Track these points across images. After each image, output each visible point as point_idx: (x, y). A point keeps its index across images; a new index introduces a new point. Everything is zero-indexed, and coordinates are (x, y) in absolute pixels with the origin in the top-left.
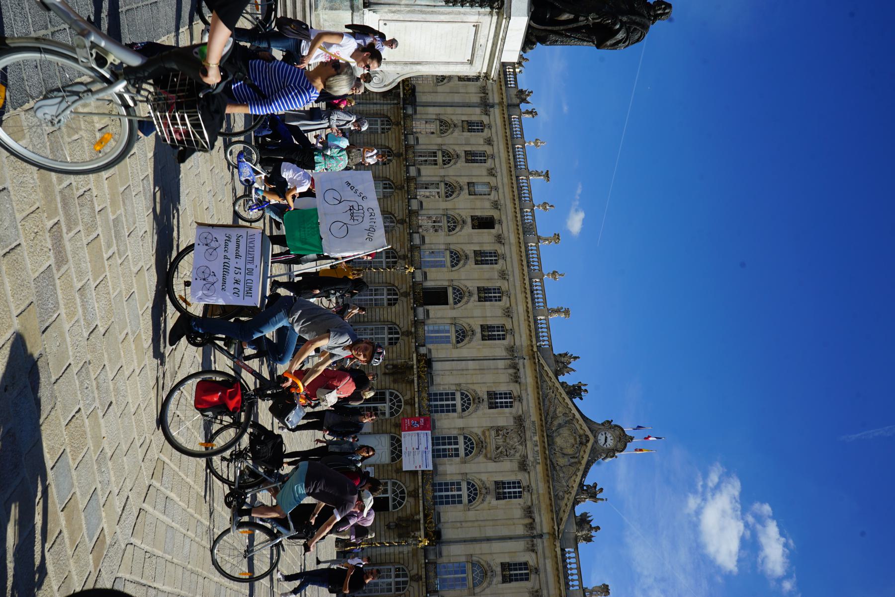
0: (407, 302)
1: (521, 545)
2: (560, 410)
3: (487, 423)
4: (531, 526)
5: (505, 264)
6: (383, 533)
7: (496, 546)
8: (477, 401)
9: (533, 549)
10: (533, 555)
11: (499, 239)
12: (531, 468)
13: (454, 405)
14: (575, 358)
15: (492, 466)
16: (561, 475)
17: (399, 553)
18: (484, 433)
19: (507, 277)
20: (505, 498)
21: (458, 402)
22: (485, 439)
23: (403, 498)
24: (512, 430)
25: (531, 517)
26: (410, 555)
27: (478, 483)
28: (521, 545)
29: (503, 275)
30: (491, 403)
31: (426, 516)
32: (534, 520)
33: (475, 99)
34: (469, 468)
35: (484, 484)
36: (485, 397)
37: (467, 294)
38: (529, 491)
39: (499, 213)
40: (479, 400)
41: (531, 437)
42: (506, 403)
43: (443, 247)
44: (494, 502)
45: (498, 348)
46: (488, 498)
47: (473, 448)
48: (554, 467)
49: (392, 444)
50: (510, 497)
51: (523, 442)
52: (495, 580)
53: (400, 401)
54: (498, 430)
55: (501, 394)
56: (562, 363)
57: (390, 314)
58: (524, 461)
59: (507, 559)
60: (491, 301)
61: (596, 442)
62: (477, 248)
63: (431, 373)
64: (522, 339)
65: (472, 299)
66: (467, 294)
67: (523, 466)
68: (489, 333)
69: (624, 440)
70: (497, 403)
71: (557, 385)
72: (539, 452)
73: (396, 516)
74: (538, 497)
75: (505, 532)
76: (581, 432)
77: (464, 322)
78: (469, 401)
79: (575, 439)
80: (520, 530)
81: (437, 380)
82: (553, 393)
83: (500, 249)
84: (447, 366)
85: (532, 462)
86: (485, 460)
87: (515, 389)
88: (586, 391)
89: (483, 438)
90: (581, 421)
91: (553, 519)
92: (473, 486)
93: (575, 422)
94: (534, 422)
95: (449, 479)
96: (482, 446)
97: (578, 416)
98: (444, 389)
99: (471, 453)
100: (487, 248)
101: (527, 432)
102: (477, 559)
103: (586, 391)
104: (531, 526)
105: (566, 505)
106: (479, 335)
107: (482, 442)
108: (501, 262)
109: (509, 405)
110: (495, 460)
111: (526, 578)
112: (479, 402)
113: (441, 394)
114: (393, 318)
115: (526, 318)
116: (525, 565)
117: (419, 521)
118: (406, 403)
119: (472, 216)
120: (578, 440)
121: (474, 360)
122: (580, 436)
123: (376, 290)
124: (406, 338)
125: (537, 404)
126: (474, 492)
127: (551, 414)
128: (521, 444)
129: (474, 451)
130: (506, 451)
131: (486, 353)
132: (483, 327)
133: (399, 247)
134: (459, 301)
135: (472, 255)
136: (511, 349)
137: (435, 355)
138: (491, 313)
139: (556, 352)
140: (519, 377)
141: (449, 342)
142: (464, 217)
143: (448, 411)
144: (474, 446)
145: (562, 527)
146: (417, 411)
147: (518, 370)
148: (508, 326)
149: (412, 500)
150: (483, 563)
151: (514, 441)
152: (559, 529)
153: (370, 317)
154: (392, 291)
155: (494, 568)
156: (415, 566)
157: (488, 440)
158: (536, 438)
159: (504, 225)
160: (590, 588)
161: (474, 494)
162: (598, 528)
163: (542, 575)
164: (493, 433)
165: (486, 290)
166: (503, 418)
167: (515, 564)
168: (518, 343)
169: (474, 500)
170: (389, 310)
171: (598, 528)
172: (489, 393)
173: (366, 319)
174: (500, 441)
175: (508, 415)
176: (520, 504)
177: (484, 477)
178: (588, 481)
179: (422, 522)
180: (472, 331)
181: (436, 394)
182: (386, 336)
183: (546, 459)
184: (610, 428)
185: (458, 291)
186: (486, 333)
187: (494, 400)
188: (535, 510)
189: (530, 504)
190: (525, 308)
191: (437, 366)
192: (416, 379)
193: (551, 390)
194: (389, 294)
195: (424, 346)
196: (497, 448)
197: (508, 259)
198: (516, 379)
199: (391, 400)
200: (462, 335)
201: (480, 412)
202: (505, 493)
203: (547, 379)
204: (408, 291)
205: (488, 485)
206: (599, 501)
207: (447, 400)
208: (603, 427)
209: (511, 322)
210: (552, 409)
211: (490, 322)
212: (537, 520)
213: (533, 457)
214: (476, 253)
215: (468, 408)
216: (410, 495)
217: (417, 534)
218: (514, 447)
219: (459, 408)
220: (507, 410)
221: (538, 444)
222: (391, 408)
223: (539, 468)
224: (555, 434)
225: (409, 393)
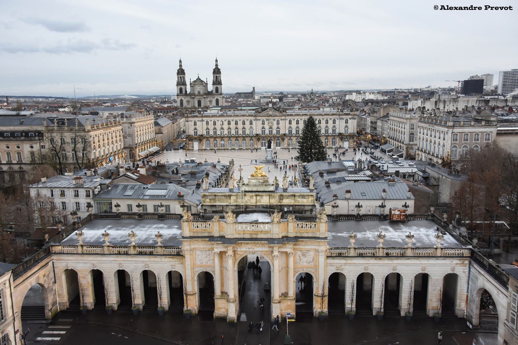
1: (286, 121)
3: (267, 125)
4: (284, 120)
11: (232, 120)
29: (240, 120)
33: (201, 122)
34: (274, 129)
45: (254, 122)
54: (268, 123)
64: (252, 118)
67: (274, 120)
68: (251, 123)
77: (249, 128)
78: (263, 128)
87: (261, 120)
104: (284, 120)
126: (278, 128)
136: (254, 120)
138: (248, 123)
144: (271, 128)
151: (270, 121)
165: (243, 123)
166: (266, 122)
187: (263, 123)
191: (257, 133)
198: (260, 120)
214: (235, 124)
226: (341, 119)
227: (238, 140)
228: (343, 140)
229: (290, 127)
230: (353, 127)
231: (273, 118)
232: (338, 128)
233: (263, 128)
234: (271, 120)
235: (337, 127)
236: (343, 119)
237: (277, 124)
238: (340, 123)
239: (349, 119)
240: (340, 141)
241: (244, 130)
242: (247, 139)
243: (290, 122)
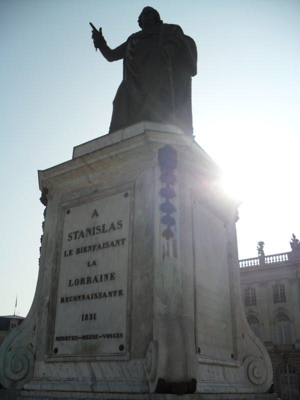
14: (294, 236)
134: (256, 319)
139: (290, 250)
180: (279, 309)
195: (294, 346)
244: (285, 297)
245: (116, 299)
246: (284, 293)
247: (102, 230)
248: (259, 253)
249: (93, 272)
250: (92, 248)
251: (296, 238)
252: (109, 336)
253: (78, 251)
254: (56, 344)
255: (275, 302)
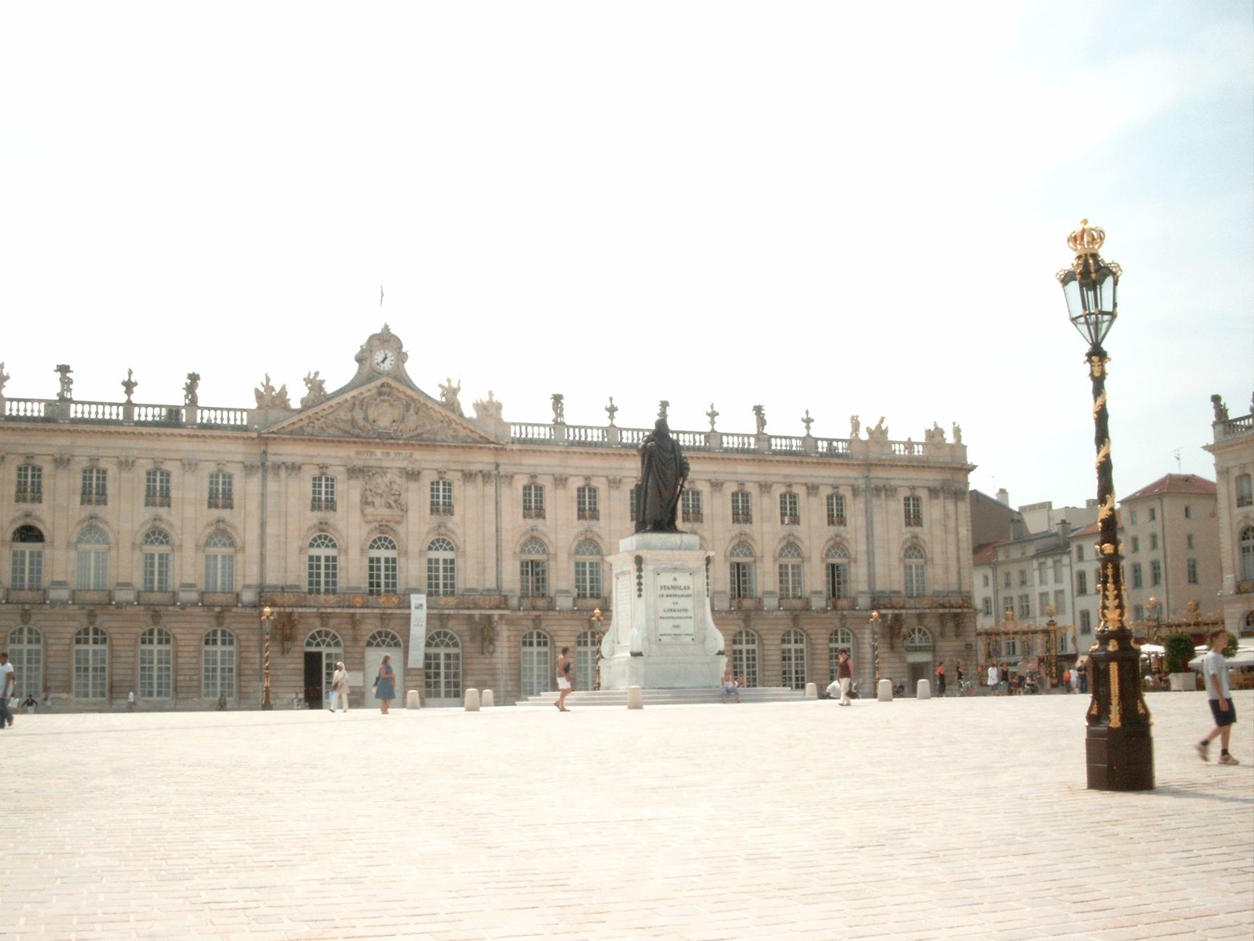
0: (168, 615)
1: (505, 491)
2: (342, 415)
3: (356, 516)
4: (486, 476)
5: (108, 459)
6: (487, 661)
7: (506, 523)
8: (324, 527)
9: (510, 478)
10: (517, 477)
12: (416, 466)
13: (327, 559)
14: (268, 380)
15: (412, 516)
16: (428, 427)
17: (509, 641)
18: (368, 522)
19: (131, 459)
20: (450, 504)
21: (323, 552)
22: (376, 521)
23: (446, 634)
24: (366, 483)
25: (476, 474)
26: (512, 628)
27: (432, 537)
28: (505, 491)
30: (326, 508)
31: (477, 607)
32: (481, 471)
34: (414, 546)
35: (434, 529)
36: (319, 515)
37: (157, 523)
38: (445, 472)
39: (13, 456)
40: (323, 526)
41: (378, 459)
42: (327, 486)
43: (73, 554)
44: (457, 517)
45: (246, 488)
46: (450, 525)
47: (386, 539)
48: (419, 435)
49: (378, 645)
50: (450, 497)
51: (383, 471)
52: (541, 528)
53: (319, 633)
54: (365, 502)
55: (314, 492)
56: (271, 400)
57: (188, 643)
58: (407, 473)
59: (521, 510)
60: (168, 488)
61: (388, 374)
62: (78, 499)
63: (283, 588)
64: (235, 452)
65: (165, 516)
66: (157, 523)
67: (414, 475)
68: (221, 497)
69: (385, 339)
70: (326, 499)
71: (310, 412)
72: (397, 451)
73: (468, 644)
74: (454, 462)
75: (491, 508)
76: (374, 391)
78: (323, 536)
79: (384, 401)
80: (490, 490)
81: (292, 580)
82: (318, 420)
83: (81, 463)
84: (271, 563)
85: (410, 462)
86: (404, 525)
87: (310, 472)
88: (317, 374)
89: (376, 524)
90: (363, 389)
91: (480, 448)
92: (433, 543)
93: (362, 397)
94: (358, 453)
95: (425, 574)
96: (386, 526)
97: (354, 393)
98: (305, 571)
99: (391, 542)
100: (78, 482)
101: (370, 464)
102: (518, 546)
103: (317, 374)
104: (486, 476)
105: (465, 428)
106: (224, 513)
107: (381, 526)
108: (103, 464)
109: (331, 482)
110: (404, 510)
111: (540, 489)
112: (326, 523)
113: (311, 575)
114: (195, 637)
115: (201, 439)
116: (527, 489)
117: (481, 615)
118: (324, 624)
119: (17, 501)
120: (386, 398)
121: (263, 524)
122: (380, 394)
123: (143, 662)
124: (227, 621)
125: (333, 444)
127: (348, 427)
128: (385, 473)
129: (390, 537)
130: (394, 495)
131: (253, 506)
132: (212, 504)
133: (71, 623)
134: (166, 536)
135: (89, 509)
136: (249, 469)
137: (253, 579)
139: (253, 405)
140: (293, 464)
141: (231, 558)
142: (17, 514)
143: (334, 567)
144: (384, 536)
145: (493, 439)
146: (338, 610)
147: (284, 463)
148: (212, 468)
149: (451, 623)
150: (522, 541)
151: (381, 482)
152: (493, 443)
153: (192, 672)
154: (147, 639)
155: (528, 527)
156: (524, 622)
157: (379, 518)
158: (379, 453)
159: (36, 450)
160: (553, 415)
161: (385, 541)
162: (491, 393)
163: (539, 470)
164: (369, 510)
166: (349, 493)
167: (525, 501)
168: (240, 458)
169: (333, 540)
170: (182, 643)
171: (491, 393)
172: (313, 508)
173: (195, 678)
174: (377, 500)
175: (346, 487)
176: (460, 487)
177: (425, 528)
178: (436, 394)
179: (483, 612)
180: (219, 521)
181: (311, 583)
182: (219, 648)
183: (406, 445)
184: (371, 351)
185: (148, 536)
186: (220, 501)
187: (324, 502)
188: (467, 468)
189: (460, 474)
190: (186, 439)
191: (272, 578)
192: (300, 610)
193: (316, 421)
194: (151, 642)
195: (238, 595)
196: (390, 506)
197: (101, 452)
198: (295, 468)
199: (318, 645)
200: (222, 534)
201: (341, 525)
202: (444, 503)
203: (299, 425)
204: (150, 613)
205: (435, 524)
206: (461, 385)
207: (318, 567)
208: (368, 363)
209: (207, 463)
210: (342, 425)
211: (206, 495)
212: (478, 467)
213: (403, 460)
215: (331, 540)
216: (443, 625)
217: (496, 618)
218: (388, 484)
219: (331, 552)
220: (339, 487)
221: (386, 451)
222: (329, 645)
223: (418, 455)
224: (376, 427)
225: (311, 620)
226: (878, 490)
227: (101, 637)
228: (898, 642)
229: (534, 540)
230: (952, 549)
231: (395, 460)
232: (862, 558)
233: (323, 536)
234: (383, 471)
235: (858, 547)
236: (889, 491)
237: (434, 509)
238: (877, 519)
239: (923, 494)
240: (883, 650)
241: (157, 549)
242: (177, 629)
243: (534, 506)
244: (230, 498)
245: (688, 620)
246: (230, 490)
247: (680, 588)
248: (186, 397)
249: (677, 607)
250: (675, 596)
251: (271, 384)
252: (687, 635)
253: (667, 596)
254: (660, 637)
255: (210, 506)
